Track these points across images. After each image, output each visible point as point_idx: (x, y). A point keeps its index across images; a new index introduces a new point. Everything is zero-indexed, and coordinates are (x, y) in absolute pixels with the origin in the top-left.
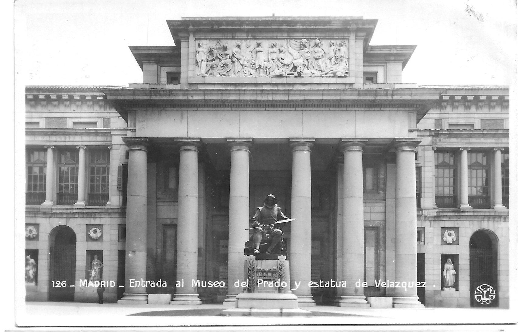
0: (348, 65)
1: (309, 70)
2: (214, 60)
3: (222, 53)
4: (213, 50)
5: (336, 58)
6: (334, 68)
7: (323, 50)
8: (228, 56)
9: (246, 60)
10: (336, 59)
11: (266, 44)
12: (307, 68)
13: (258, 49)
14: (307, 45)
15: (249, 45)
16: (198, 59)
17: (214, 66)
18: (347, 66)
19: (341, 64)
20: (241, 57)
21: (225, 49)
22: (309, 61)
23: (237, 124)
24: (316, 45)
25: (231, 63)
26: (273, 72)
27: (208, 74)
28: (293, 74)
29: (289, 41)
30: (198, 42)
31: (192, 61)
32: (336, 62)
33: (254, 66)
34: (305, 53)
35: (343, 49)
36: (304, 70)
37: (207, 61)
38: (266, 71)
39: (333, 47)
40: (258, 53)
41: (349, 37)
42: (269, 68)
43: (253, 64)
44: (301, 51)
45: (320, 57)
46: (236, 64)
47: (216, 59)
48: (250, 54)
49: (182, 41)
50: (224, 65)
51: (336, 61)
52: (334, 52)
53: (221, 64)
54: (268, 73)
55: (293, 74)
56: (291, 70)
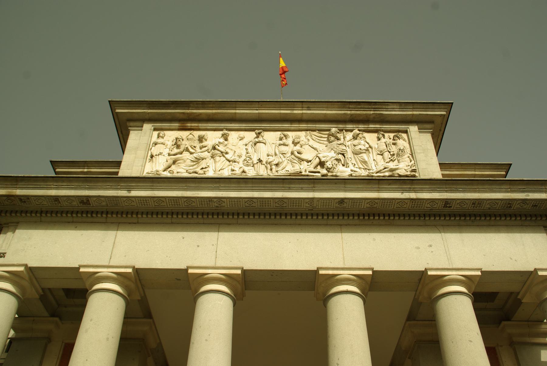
0: (413, 162)
1: (347, 167)
2: (181, 153)
3: (195, 145)
4: (181, 140)
5: (392, 153)
6: (392, 165)
7: (368, 143)
8: (206, 148)
9: (237, 154)
10: (391, 155)
11: (271, 137)
12: (343, 165)
13: (257, 140)
14: (340, 136)
15: (242, 136)
16: (155, 150)
17: (179, 162)
18: (413, 162)
19: (401, 161)
20: (228, 150)
21: (201, 139)
22: (345, 155)
23: (213, 245)
24: (355, 138)
25: (210, 158)
26: (285, 170)
27: (168, 172)
28: (319, 172)
29: (310, 133)
30: (156, 133)
31: (141, 153)
32: (392, 158)
33: (249, 161)
34: (338, 145)
35: (402, 143)
36: (338, 166)
37: (169, 155)
38: (271, 170)
39: (383, 140)
40: (258, 144)
41: (409, 128)
42: (277, 165)
43: (248, 159)
44: (331, 144)
45: (364, 151)
46: (217, 158)
47: (184, 152)
48: (245, 147)
49: (131, 132)
50: (195, 158)
51: (391, 157)
52: (387, 146)
53: (191, 157)
54: (274, 170)
55: (319, 172)
56: (316, 167)
